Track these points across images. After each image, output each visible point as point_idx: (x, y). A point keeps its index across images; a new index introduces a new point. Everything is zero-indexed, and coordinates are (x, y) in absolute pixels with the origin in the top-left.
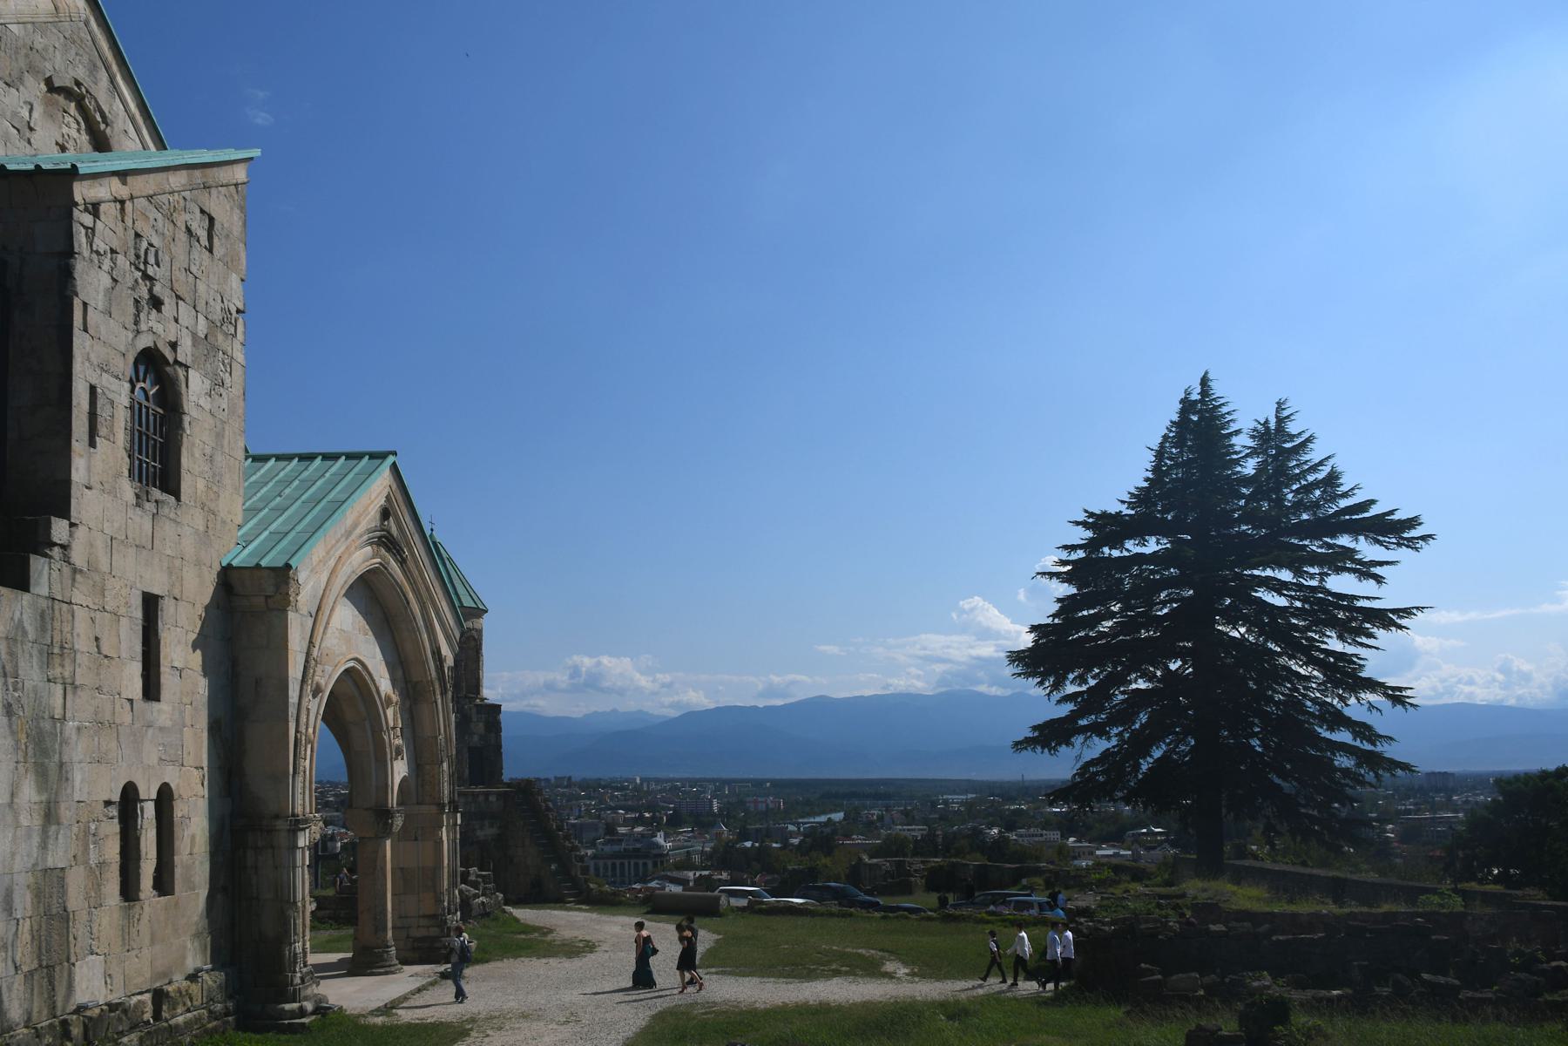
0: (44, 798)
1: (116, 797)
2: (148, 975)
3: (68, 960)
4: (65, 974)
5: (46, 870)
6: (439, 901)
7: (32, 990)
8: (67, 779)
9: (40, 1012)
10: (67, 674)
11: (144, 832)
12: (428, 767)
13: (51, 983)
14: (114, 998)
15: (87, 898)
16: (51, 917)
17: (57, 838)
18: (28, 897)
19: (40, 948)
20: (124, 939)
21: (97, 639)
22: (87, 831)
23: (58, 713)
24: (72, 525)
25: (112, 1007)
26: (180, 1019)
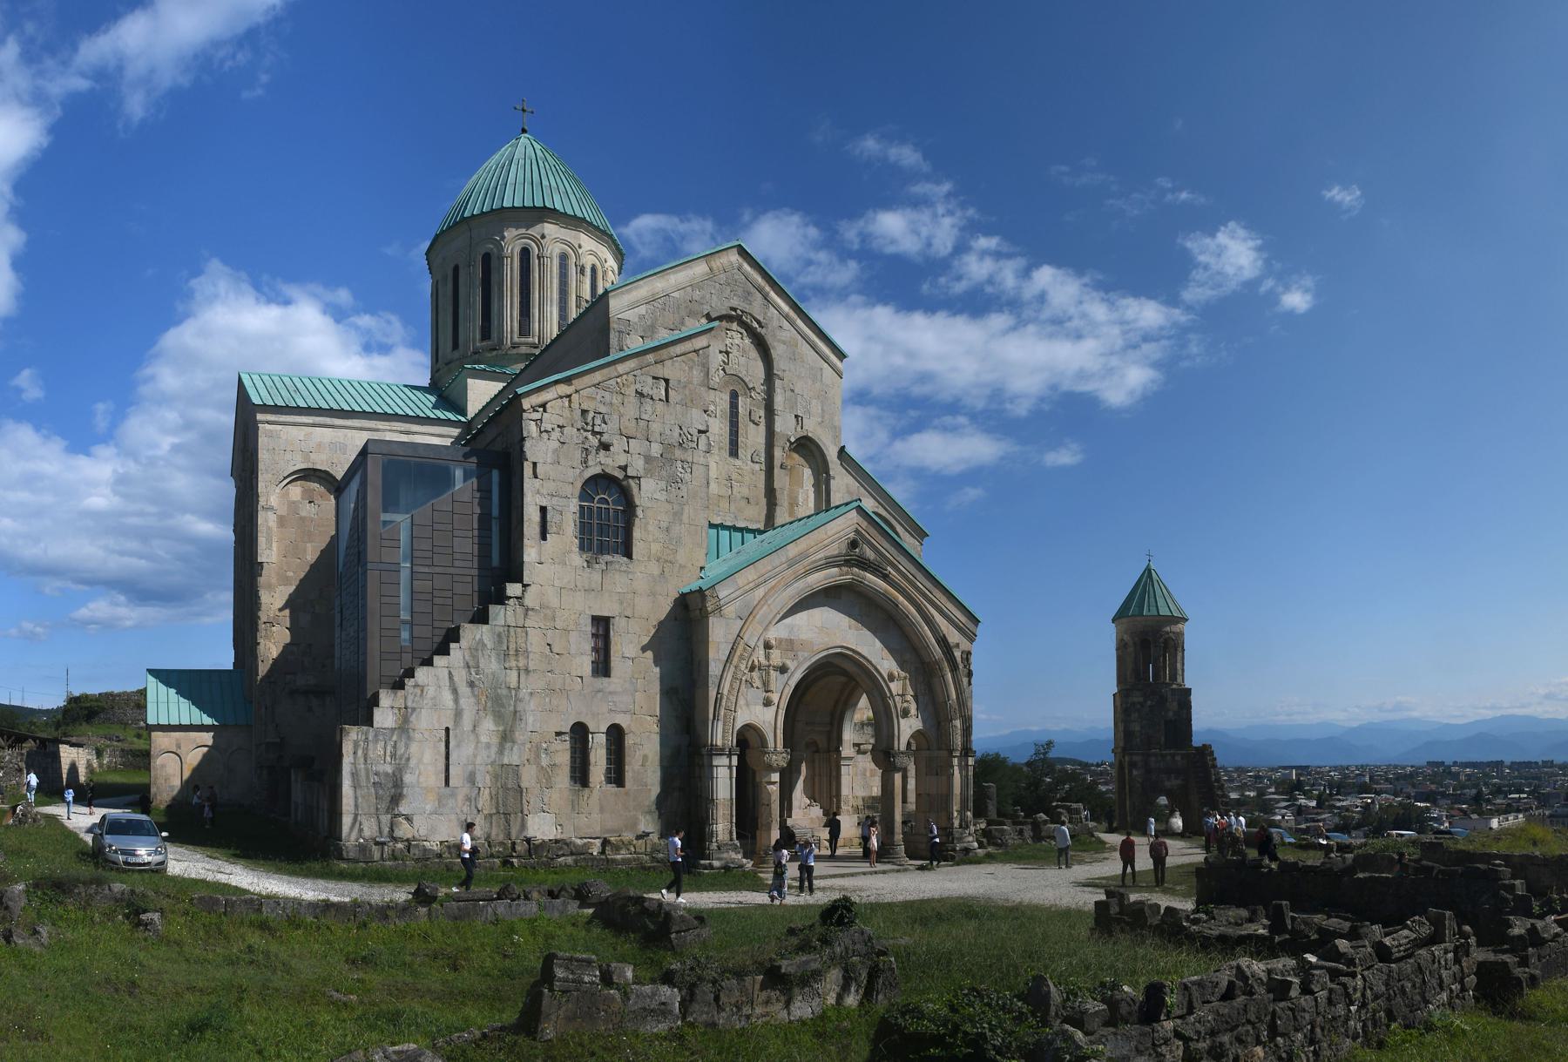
0: (501, 728)
1: (568, 731)
2: (598, 829)
3: (522, 812)
4: (519, 820)
5: (503, 765)
6: (950, 818)
7: (491, 823)
8: (521, 720)
9: (497, 835)
10: (521, 665)
11: (593, 750)
12: (943, 724)
13: (508, 821)
14: (559, 837)
15: (539, 782)
16: (508, 789)
17: (512, 749)
18: (488, 777)
19: (497, 803)
20: (573, 807)
21: (549, 645)
22: (538, 747)
23: (514, 684)
24: (525, 586)
25: (557, 841)
26: (619, 857)
